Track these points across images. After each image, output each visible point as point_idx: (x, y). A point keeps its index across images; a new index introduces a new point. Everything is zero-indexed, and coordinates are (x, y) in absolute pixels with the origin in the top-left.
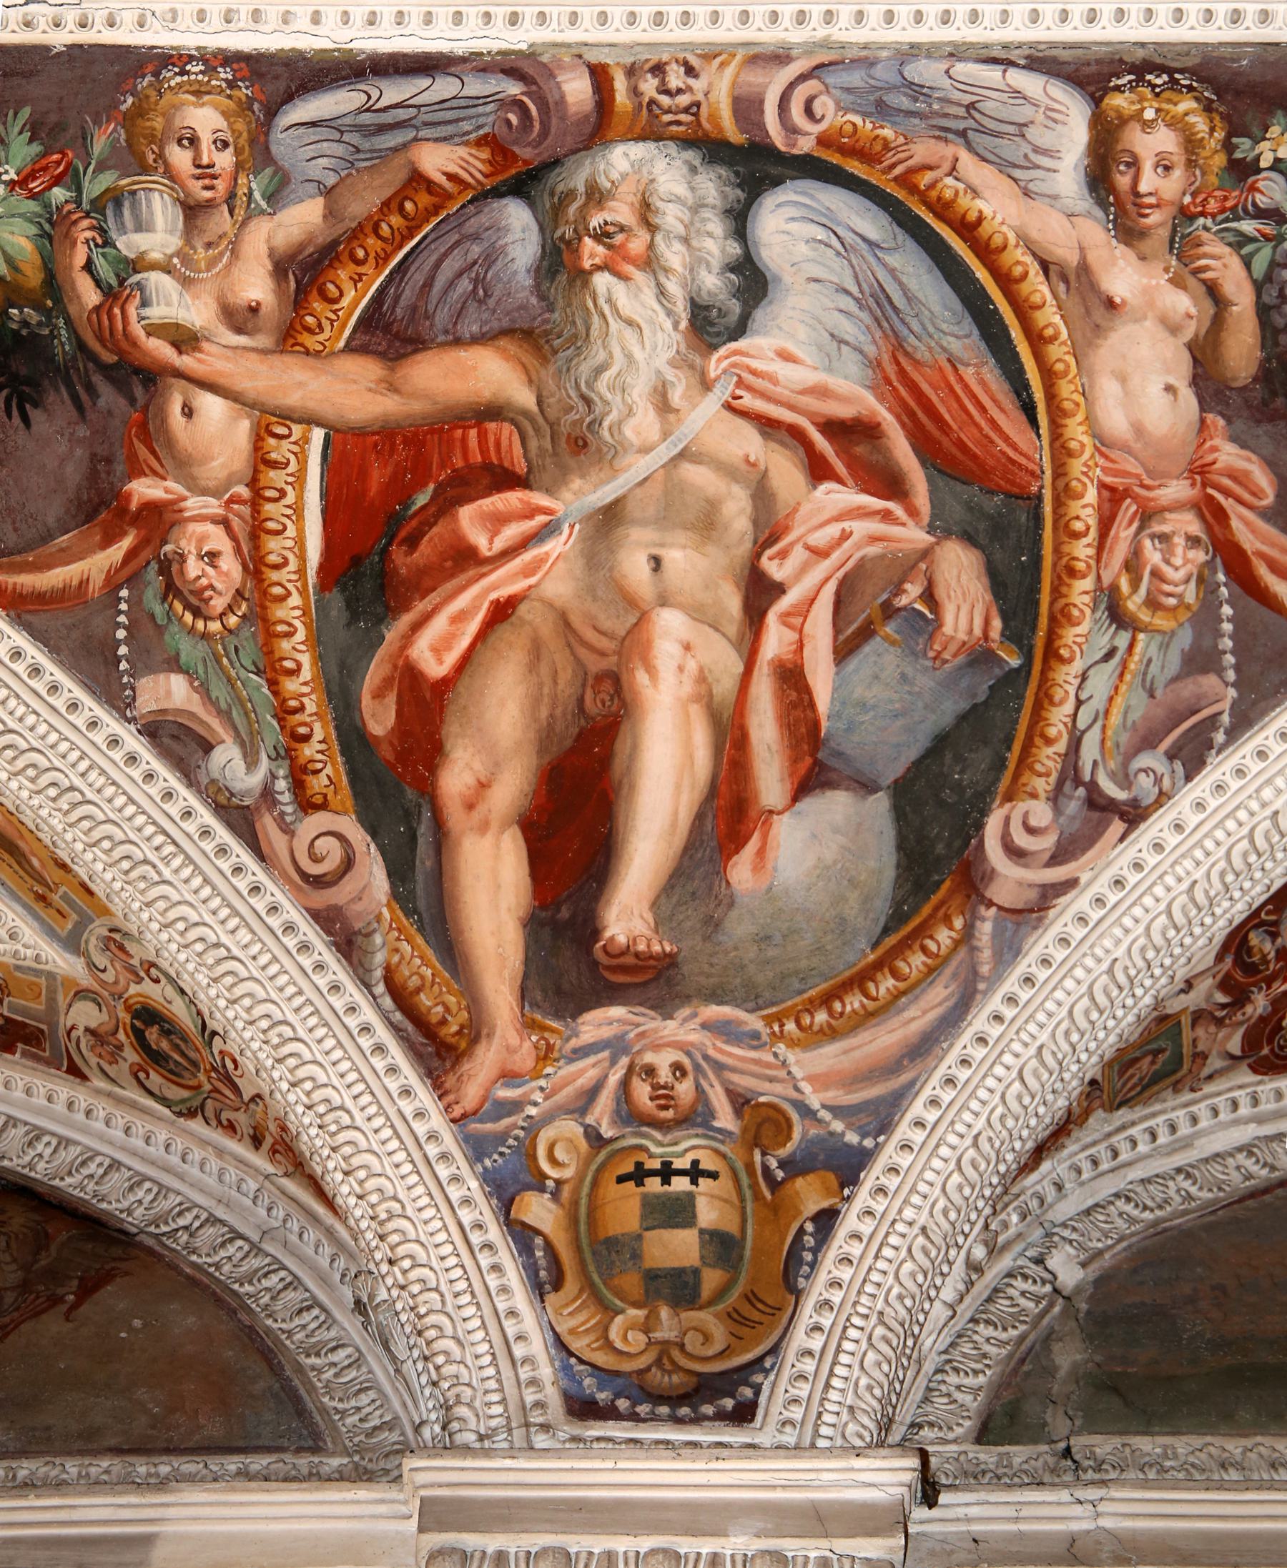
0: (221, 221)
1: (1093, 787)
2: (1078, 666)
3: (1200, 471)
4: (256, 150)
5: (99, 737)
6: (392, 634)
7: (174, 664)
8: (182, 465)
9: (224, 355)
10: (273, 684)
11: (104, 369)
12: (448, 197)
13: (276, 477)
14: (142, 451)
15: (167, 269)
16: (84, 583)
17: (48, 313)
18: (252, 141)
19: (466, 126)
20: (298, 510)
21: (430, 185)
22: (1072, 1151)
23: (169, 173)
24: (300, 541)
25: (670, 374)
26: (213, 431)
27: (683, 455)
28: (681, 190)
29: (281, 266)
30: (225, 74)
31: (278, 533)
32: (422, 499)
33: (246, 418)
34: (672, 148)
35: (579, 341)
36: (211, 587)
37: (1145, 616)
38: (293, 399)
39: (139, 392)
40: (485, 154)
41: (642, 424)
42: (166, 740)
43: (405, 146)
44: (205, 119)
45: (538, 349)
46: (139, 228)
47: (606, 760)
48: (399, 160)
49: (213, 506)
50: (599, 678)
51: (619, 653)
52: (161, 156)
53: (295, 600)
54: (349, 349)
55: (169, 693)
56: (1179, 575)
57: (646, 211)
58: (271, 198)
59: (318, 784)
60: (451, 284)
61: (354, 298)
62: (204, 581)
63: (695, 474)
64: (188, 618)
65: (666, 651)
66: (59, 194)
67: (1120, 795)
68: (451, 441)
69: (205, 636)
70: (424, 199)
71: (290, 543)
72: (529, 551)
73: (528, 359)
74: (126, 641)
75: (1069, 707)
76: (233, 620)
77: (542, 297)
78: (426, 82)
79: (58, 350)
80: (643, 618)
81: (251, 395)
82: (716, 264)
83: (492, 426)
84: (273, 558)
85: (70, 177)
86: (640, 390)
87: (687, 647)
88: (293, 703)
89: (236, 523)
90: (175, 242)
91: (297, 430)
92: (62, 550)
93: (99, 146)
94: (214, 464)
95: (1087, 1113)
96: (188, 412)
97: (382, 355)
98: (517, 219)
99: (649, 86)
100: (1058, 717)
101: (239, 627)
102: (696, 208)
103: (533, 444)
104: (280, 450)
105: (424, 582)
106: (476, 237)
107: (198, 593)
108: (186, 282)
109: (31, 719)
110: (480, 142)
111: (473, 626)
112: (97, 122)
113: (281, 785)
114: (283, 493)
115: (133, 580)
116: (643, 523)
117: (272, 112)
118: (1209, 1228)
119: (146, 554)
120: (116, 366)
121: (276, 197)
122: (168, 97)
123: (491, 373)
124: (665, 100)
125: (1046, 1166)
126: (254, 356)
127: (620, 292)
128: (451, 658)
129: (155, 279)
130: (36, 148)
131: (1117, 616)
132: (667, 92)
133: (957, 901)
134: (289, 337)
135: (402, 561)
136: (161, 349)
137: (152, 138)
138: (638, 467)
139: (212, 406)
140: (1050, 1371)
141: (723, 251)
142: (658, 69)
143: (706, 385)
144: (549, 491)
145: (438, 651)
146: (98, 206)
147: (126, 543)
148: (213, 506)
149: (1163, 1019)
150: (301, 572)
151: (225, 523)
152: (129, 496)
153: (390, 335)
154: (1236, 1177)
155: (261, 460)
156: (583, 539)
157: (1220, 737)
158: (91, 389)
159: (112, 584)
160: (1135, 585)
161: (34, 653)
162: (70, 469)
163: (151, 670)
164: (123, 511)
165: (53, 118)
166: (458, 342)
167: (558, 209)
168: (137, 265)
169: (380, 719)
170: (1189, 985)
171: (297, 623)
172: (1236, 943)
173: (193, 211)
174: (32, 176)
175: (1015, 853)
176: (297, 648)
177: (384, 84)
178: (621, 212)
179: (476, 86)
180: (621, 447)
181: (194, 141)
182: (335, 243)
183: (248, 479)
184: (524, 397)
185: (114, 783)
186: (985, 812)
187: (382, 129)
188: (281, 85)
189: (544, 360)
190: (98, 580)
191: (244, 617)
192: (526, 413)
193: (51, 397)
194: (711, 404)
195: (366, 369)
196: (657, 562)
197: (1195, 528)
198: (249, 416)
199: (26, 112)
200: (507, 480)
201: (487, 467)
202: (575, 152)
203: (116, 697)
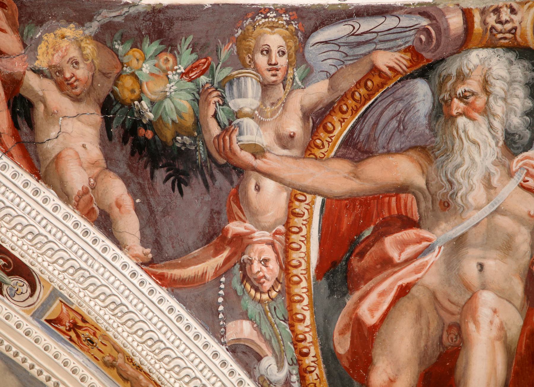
0: (279, 92)
4: (298, 56)
5: (209, 352)
6: (350, 301)
7: (245, 316)
8: (254, 215)
9: (278, 160)
10: (292, 326)
11: (220, 167)
12: (389, 78)
13: (298, 221)
14: (235, 208)
15: (252, 116)
16: (204, 274)
17: (195, 139)
18: (296, 51)
19: (400, 42)
20: (307, 238)
21: (380, 73)
23: (256, 68)
24: (308, 254)
25: (493, 169)
26: (269, 198)
27: (497, 211)
28: (504, 73)
29: (305, 116)
30: (286, 17)
31: (297, 250)
32: (367, 233)
33: (286, 191)
34: (501, 51)
35: (448, 152)
36: (264, 277)
38: (308, 182)
39: (235, 178)
40: (408, 56)
41: (477, 195)
42: (240, 354)
43: (370, 53)
44: (275, 40)
45: (428, 156)
46: (240, 96)
47: (452, 369)
48: (366, 60)
49: (267, 236)
50: (450, 327)
51: (461, 314)
52: (252, 59)
53: (304, 284)
54: (336, 156)
55: (242, 330)
57: (486, 85)
58: (303, 80)
59: (312, 378)
60: (387, 123)
61: (340, 131)
62: (261, 274)
63: (503, 221)
64: (253, 292)
65: (484, 313)
66: (203, 79)
68: (383, 204)
69: (260, 301)
70: (377, 80)
71: (303, 255)
72: (417, 260)
73: (423, 161)
74: (223, 304)
76: (274, 294)
77: (432, 130)
78: (381, 20)
79: (198, 157)
80: (473, 296)
81: (288, 180)
82: (519, 112)
83: (403, 196)
84: (294, 263)
85: (208, 70)
86: (477, 177)
87: (495, 311)
88: (301, 337)
89: (277, 244)
90: (256, 103)
91: (309, 197)
92: (195, 257)
93: (224, 55)
94: (269, 214)
96: (258, 188)
97: (352, 159)
98: (421, 89)
99: (491, 19)
101: (276, 297)
102: (511, 83)
103: (423, 205)
104: (300, 208)
105: (366, 276)
106: (401, 99)
107: (258, 280)
108: (261, 123)
109: (177, 342)
110: (407, 50)
111: (389, 299)
112: (224, 43)
113: (294, 378)
114: (301, 229)
115: (228, 273)
116: (475, 246)
117: (307, 37)
119: (234, 260)
120: (225, 165)
121: (305, 80)
122: (258, 29)
123: (402, 169)
124: (499, 27)
126: (291, 160)
127: (470, 126)
128: (378, 315)
129: (246, 122)
130: (194, 56)
132: (501, 22)
134: (308, 150)
135: (357, 264)
136: (246, 157)
137: (249, 51)
138: (474, 217)
139: (269, 185)
141: (523, 105)
142: (497, 11)
143: (511, 175)
144: (430, 230)
145: (372, 311)
146: (221, 85)
147: (225, 254)
148: (267, 236)
150: (308, 269)
151: (272, 244)
152: (227, 231)
153: (356, 149)
155: (291, 213)
156: (445, 254)
158: (212, 176)
159: (217, 276)
161: (180, 309)
162: (201, 216)
163: (234, 318)
164: (224, 238)
165: (203, 41)
166: (389, 153)
167: (442, 85)
168: (238, 115)
169: (342, 345)
171: (304, 295)
173: (266, 87)
174: (191, 70)
176: (304, 309)
177: (361, 21)
178: (473, 85)
179: (406, 21)
180: (466, 207)
181: (268, 52)
182: (333, 103)
183: (284, 223)
184: (420, 181)
185: (216, 376)
187: (359, 44)
188: (312, 23)
189: (431, 162)
190: (211, 273)
191: (279, 292)
192: (420, 189)
193: (194, 181)
194: (513, 184)
195: (344, 167)
196: (481, 266)
198: (287, 190)
199: (190, 38)
200: (409, 223)
201: (400, 216)
202: (452, 54)
203: (218, 334)
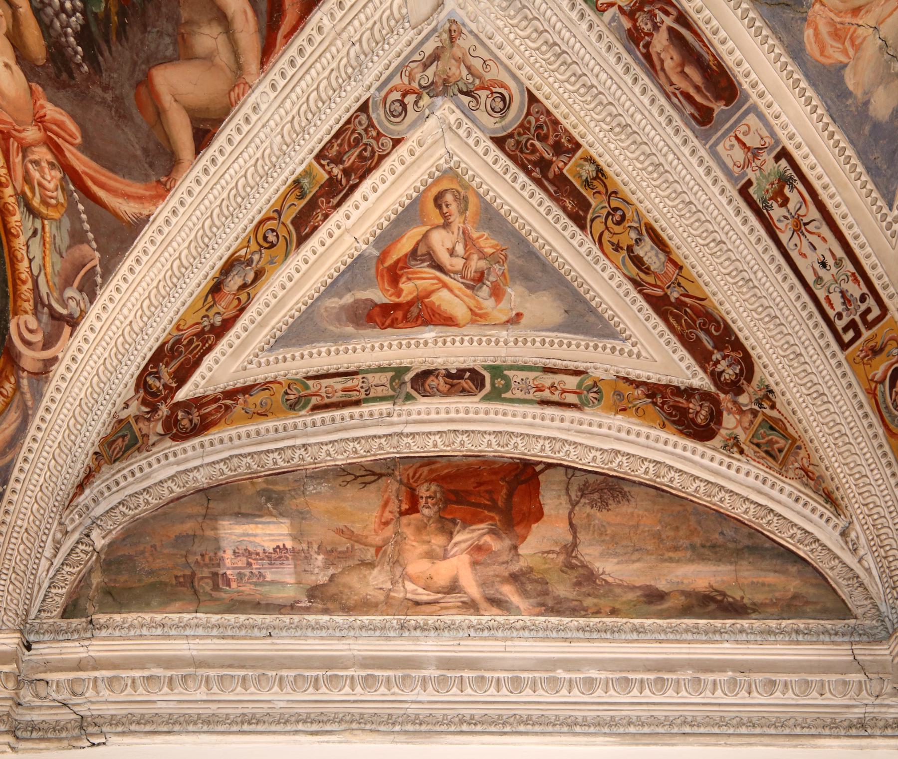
1: (50, 307)
2: (22, 239)
3: (40, 120)
22: (98, 485)
37: (43, 210)
56: (51, 186)
67: (64, 312)
75: (26, 263)
95: (99, 467)
100: (23, 266)
118: (154, 518)
125: (87, 491)
131: (31, 210)
133: (8, 369)
140: (89, 586)
149: (120, 421)
154: (166, 492)
157: (99, 280)
160: (32, 190)
170: (127, 405)
172: (141, 383)
175: (27, 343)
186: (7, 322)
197: (50, 157)
